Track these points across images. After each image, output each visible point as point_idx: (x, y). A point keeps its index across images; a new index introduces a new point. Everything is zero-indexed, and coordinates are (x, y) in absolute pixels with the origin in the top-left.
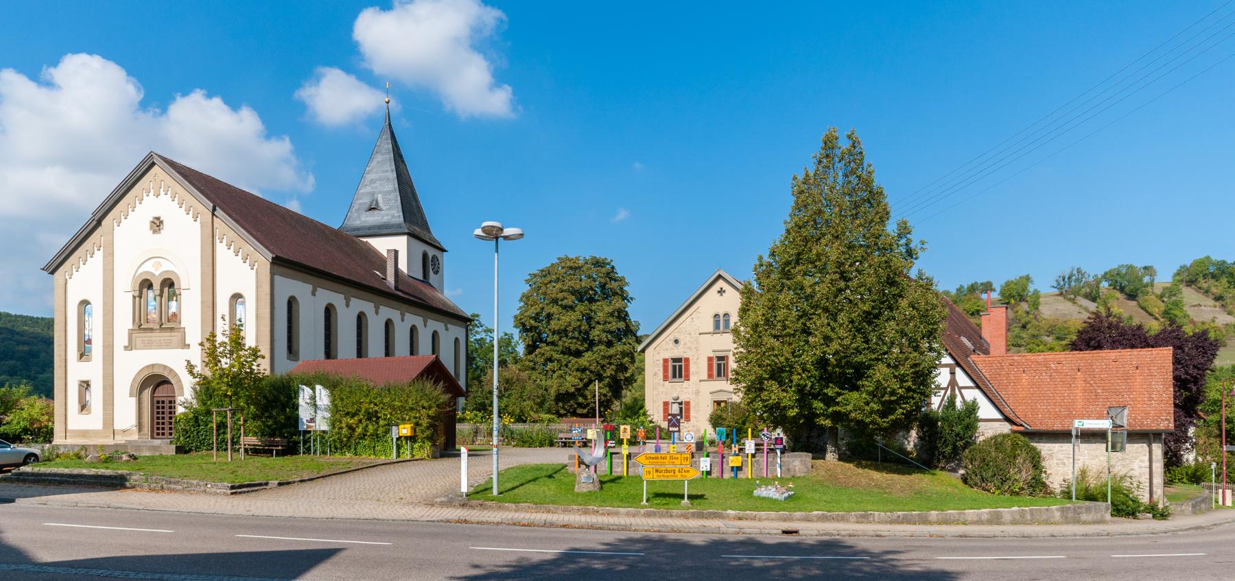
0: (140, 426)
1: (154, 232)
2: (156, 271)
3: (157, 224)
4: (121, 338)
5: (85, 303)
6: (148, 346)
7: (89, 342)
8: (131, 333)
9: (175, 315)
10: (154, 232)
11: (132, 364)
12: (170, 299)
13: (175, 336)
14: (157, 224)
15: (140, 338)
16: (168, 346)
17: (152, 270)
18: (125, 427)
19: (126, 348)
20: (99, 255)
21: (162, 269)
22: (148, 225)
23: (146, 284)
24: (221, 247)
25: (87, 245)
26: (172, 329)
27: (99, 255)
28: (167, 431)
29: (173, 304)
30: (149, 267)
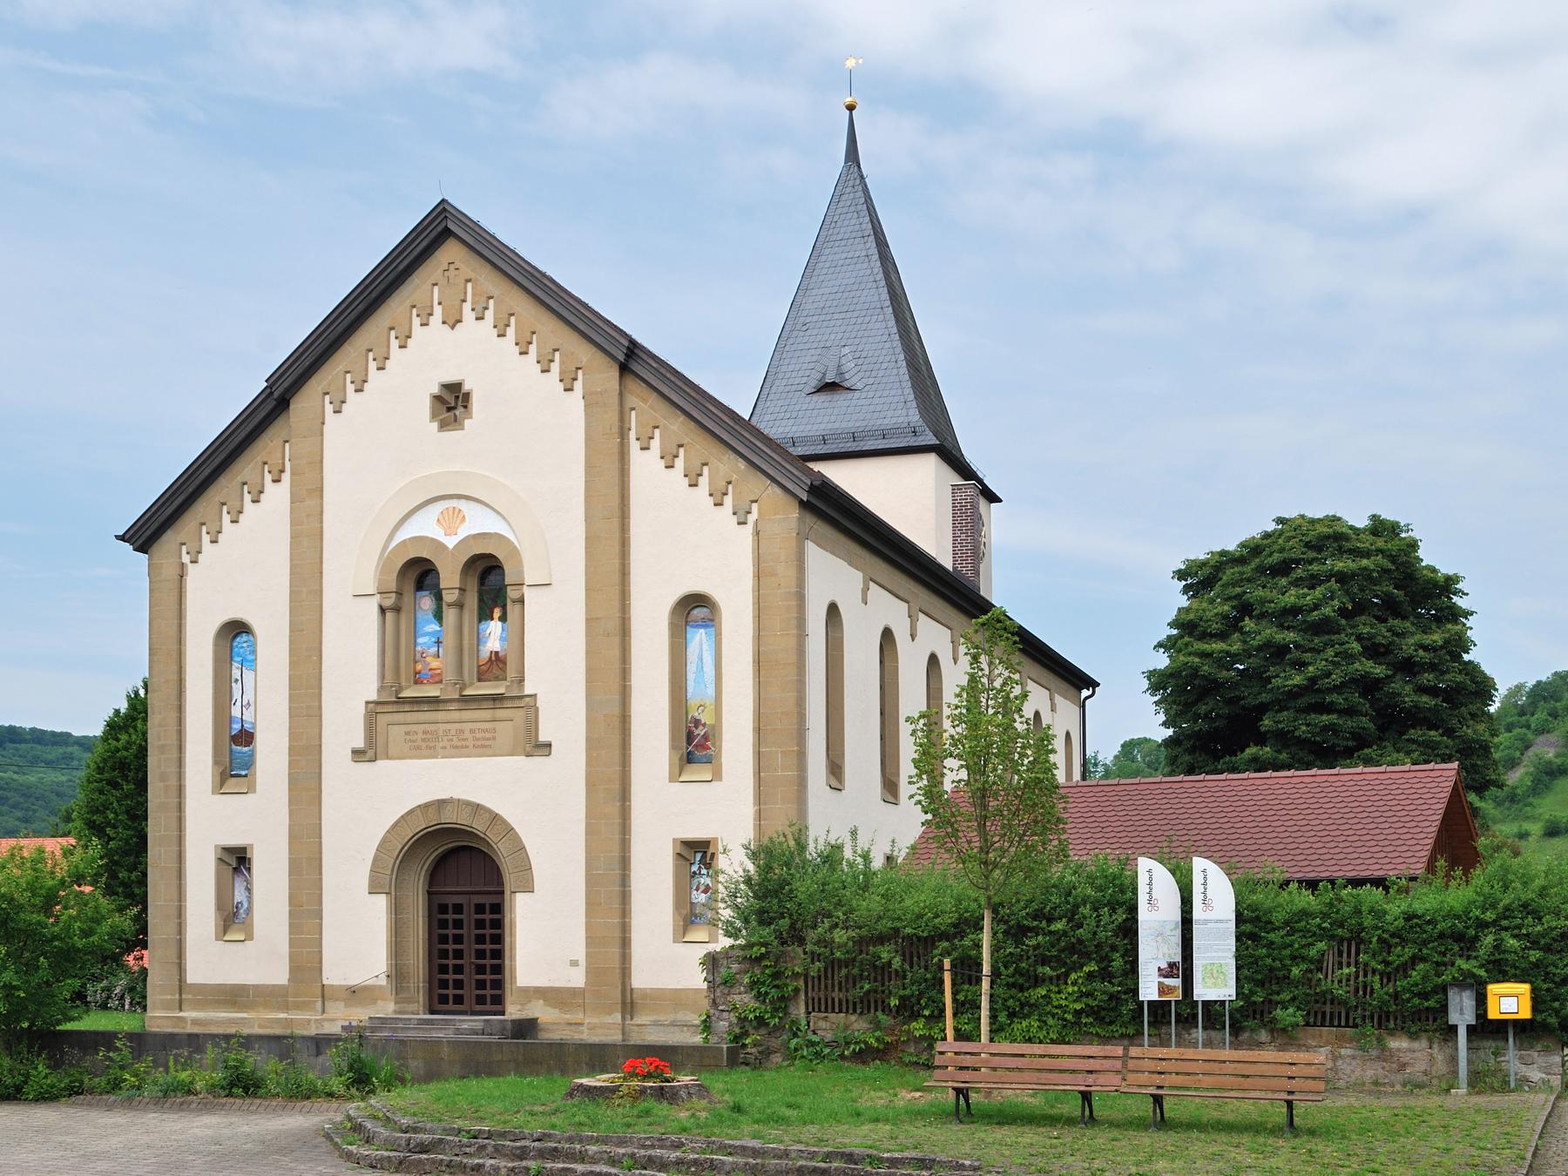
0: (398, 974)
1: (443, 426)
2: (447, 535)
3: (452, 402)
4: (343, 724)
5: (236, 630)
6: (425, 748)
7: (245, 737)
8: (374, 710)
9: (497, 660)
10: (443, 426)
11: (374, 801)
12: (485, 615)
13: (508, 723)
14: (452, 402)
15: (395, 729)
16: (484, 747)
17: (437, 533)
18: (355, 979)
19: (358, 754)
20: (278, 496)
21: (464, 531)
22: (426, 405)
23: (419, 573)
24: (645, 465)
25: (245, 469)
26: (496, 699)
27: (278, 496)
28: (469, 992)
29: (494, 628)
30: (427, 526)
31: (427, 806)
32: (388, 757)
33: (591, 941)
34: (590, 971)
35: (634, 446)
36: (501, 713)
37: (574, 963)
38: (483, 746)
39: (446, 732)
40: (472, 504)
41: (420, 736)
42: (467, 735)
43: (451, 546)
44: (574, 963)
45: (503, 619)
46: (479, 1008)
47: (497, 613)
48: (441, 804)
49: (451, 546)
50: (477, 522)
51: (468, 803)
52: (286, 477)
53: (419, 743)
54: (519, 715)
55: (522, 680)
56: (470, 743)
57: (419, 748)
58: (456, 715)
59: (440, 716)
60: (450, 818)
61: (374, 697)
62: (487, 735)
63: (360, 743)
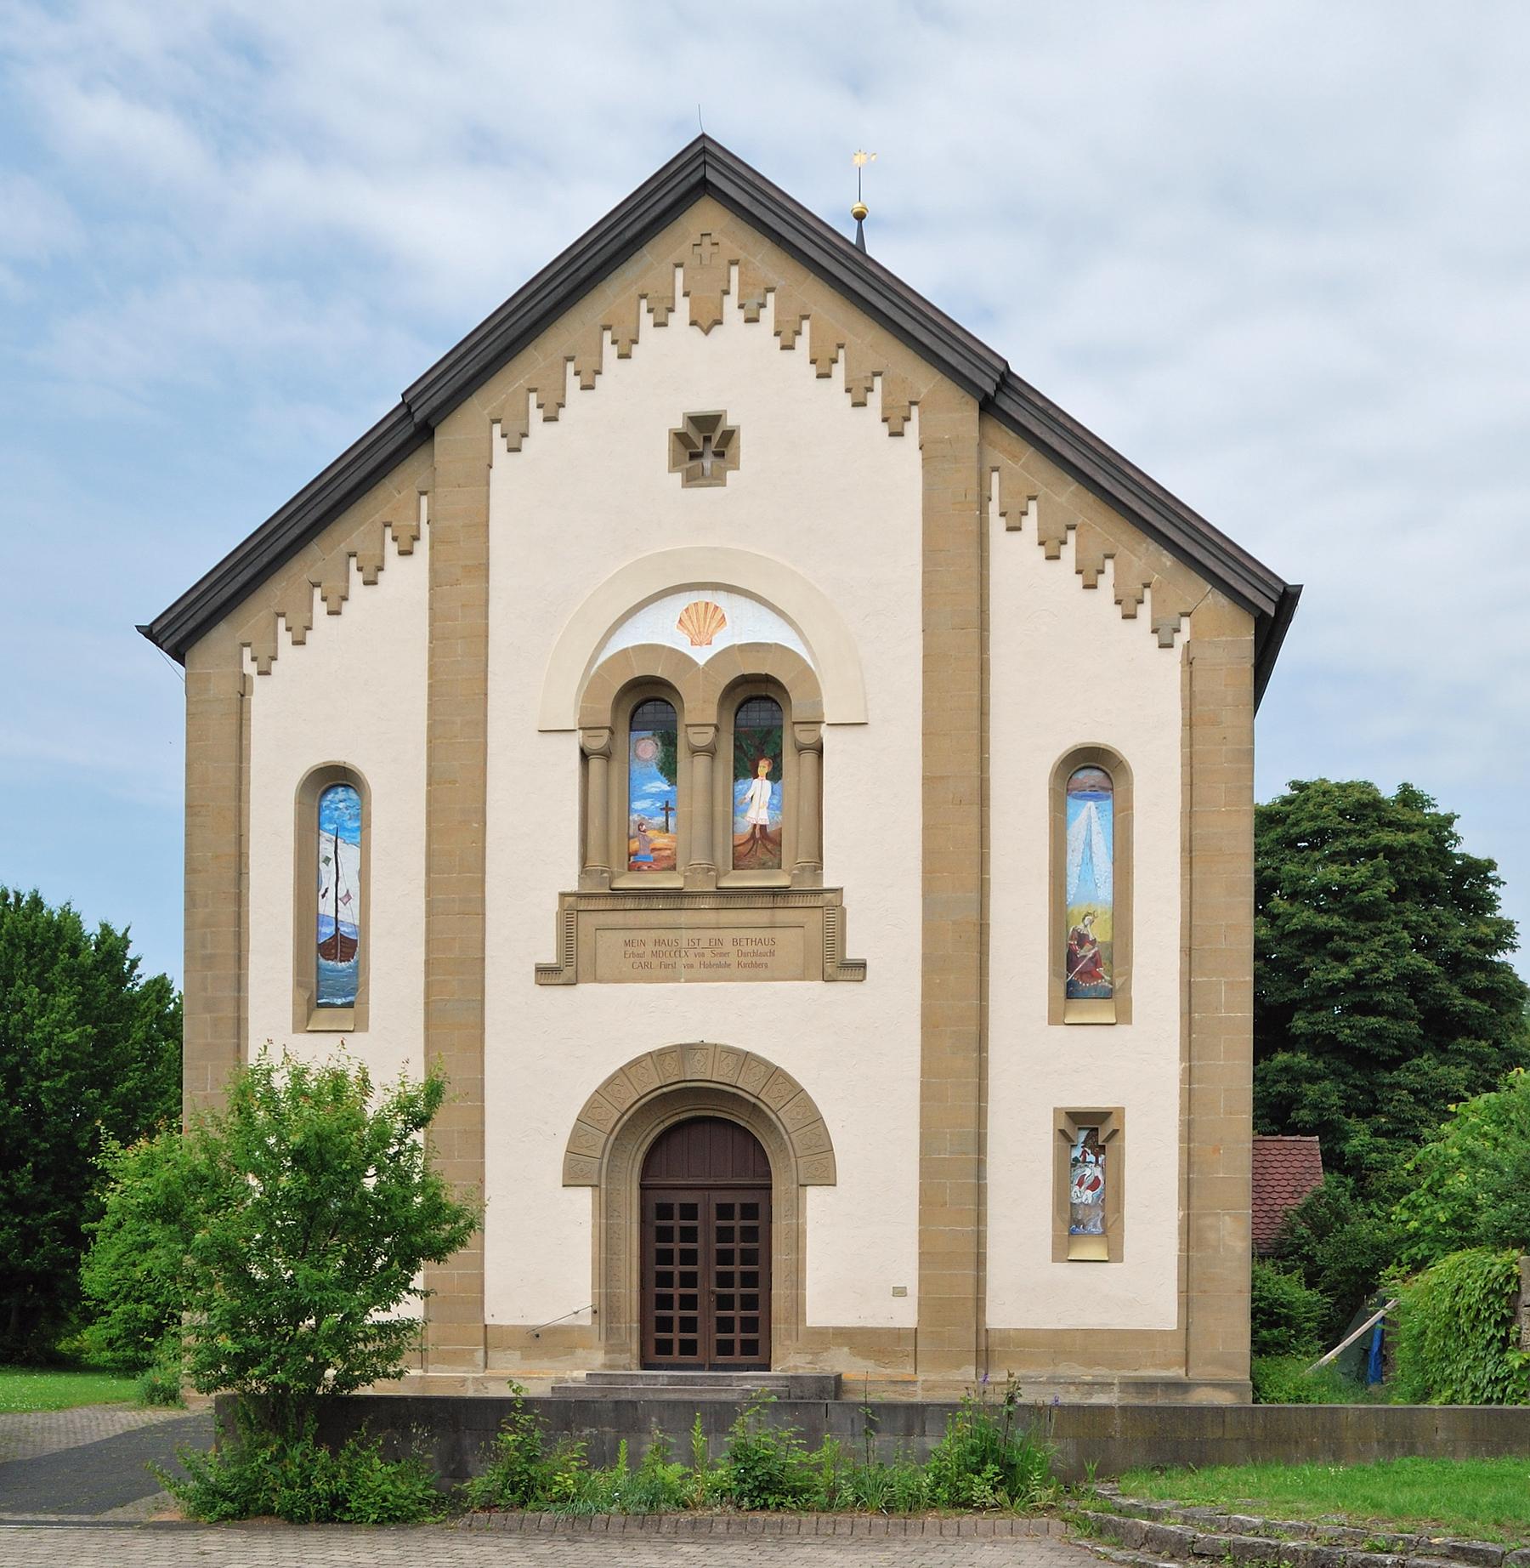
0: (605, 1309)
1: (691, 479)
2: (699, 643)
3: (704, 444)
5: (334, 778)
6: (658, 966)
7: (343, 946)
8: (572, 908)
9: (764, 843)
10: (691, 479)
12: (744, 769)
13: (795, 932)
14: (704, 444)
15: (609, 936)
16: (756, 967)
17: (680, 642)
18: (542, 1317)
19: (546, 974)
20: (407, 579)
21: (723, 640)
22: (663, 446)
23: (646, 701)
24: (1015, 555)
25: (353, 531)
26: (775, 893)
27: (407, 579)
28: (706, 1336)
29: (759, 790)
30: (661, 629)
31: (662, 1053)
32: (596, 980)
33: (926, 1258)
34: (925, 1304)
35: (997, 525)
36: (782, 916)
37: (900, 1292)
38: (757, 965)
39: (694, 943)
40: (735, 598)
41: (650, 947)
42: (728, 947)
43: (701, 662)
44: (900, 1292)
45: (775, 775)
46: (722, 1359)
47: (764, 767)
48: (685, 1051)
49: (701, 662)
50: (743, 626)
51: (730, 1051)
52: (422, 548)
53: (648, 958)
54: (813, 919)
55: (818, 866)
56: (733, 959)
57: (647, 965)
58: (711, 917)
59: (683, 918)
60: (700, 1072)
61: (573, 886)
62: (761, 948)
63: (550, 957)
